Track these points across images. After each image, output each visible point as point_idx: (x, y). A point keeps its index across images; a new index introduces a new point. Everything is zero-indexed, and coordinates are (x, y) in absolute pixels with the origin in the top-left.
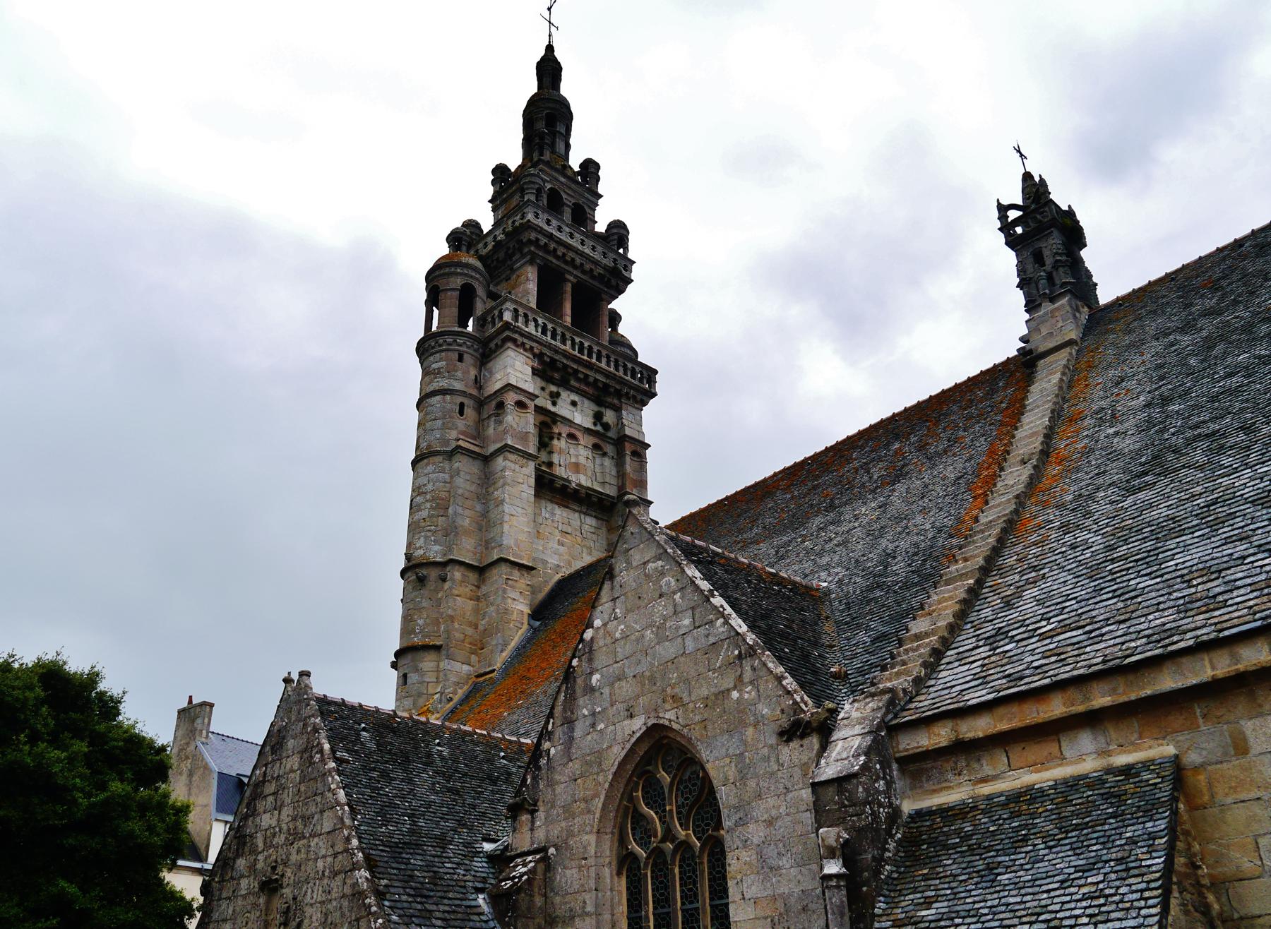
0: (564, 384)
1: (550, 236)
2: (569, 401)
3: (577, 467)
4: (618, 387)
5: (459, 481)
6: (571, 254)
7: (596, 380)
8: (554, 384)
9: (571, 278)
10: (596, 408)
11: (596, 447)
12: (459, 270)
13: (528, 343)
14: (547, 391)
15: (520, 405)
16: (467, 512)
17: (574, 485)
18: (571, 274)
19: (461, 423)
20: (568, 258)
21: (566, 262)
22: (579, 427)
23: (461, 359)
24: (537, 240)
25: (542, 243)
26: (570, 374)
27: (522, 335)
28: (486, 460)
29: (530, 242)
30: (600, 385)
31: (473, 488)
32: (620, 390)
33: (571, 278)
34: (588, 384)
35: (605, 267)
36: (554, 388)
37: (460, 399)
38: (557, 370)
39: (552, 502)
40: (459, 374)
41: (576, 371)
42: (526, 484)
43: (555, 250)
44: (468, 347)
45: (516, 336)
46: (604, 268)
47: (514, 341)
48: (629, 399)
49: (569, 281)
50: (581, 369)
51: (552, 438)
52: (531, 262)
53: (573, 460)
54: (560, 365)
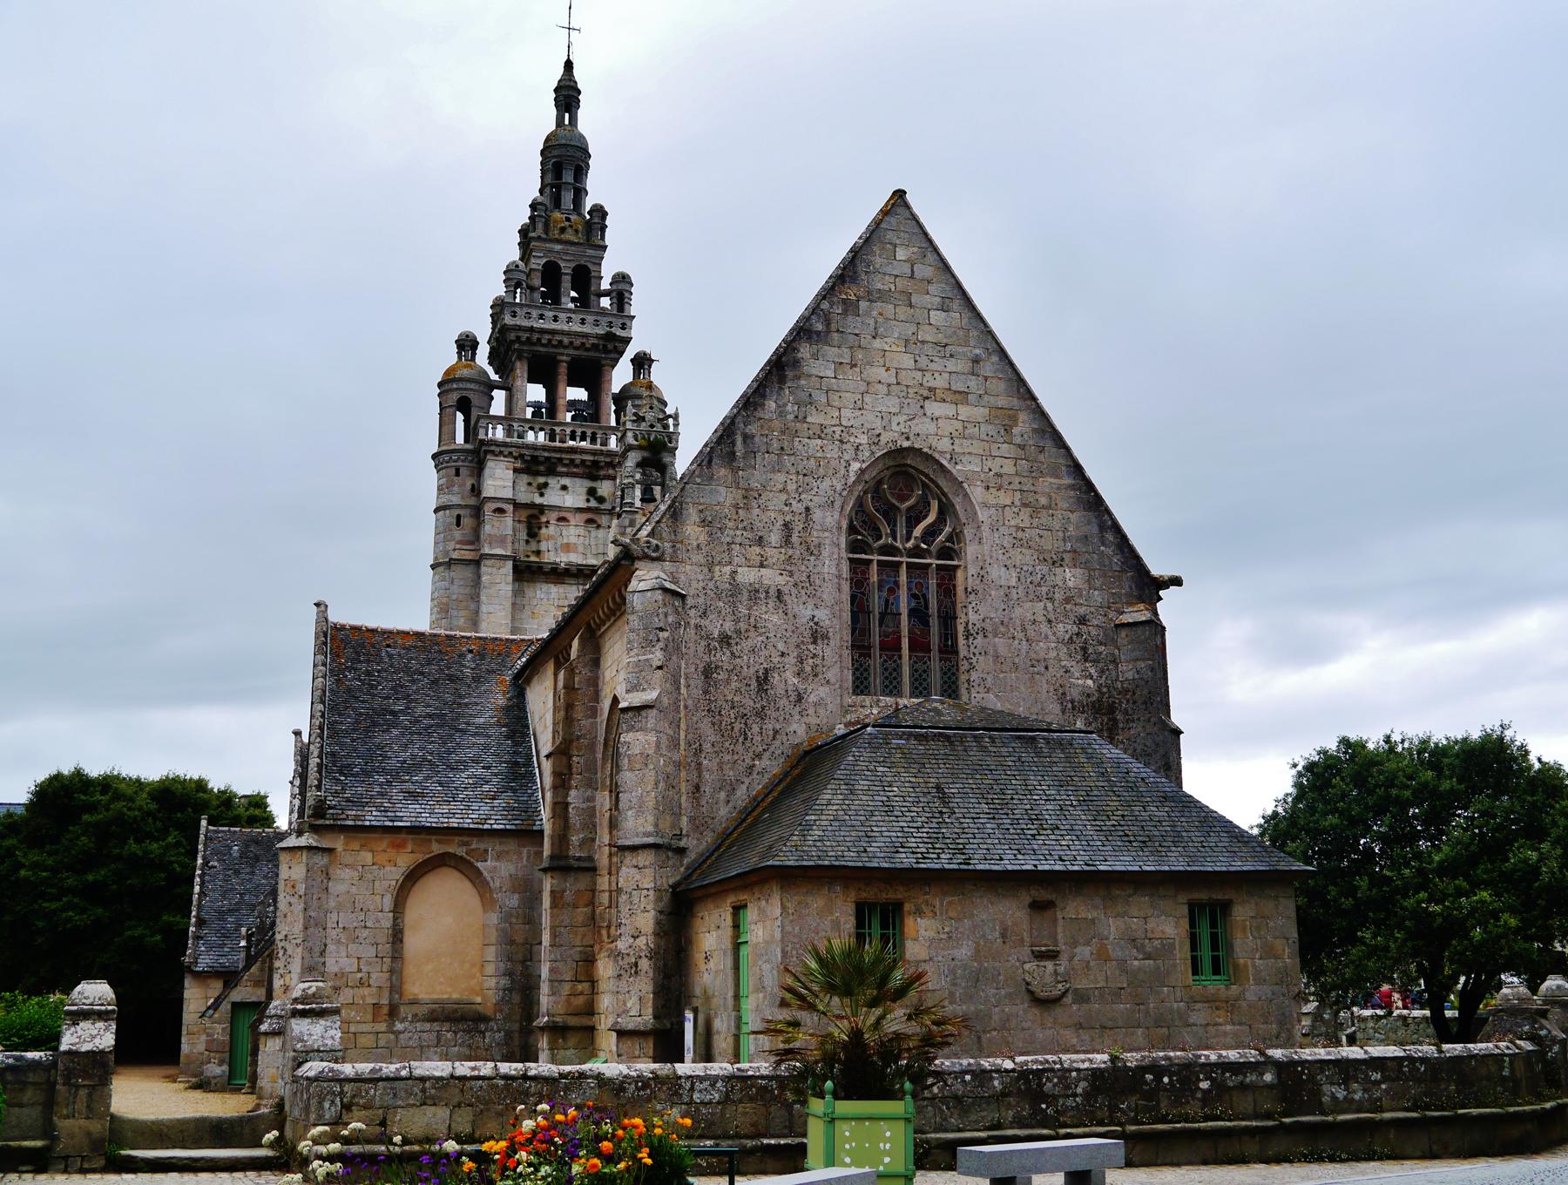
0: (552, 472)
1: (532, 329)
2: (559, 486)
3: (567, 548)
4: (608, 460)
5: (455, 588)
6: (558, 338)
7: (583, 461)
8: (541, 475)
9: (565, 358)
10: (588, 484)
11: (589, 521)
12: (455, 386)
13: (506, 451)
14: (535, 485)
15: (500, 511)
16: (462, 613)
17: (563, 565)
18: (562, 354)
19: (458, 534)
20: (554, 343)
21: (555, 347)
22: (569, 510)
23: (457, 474)
24: (518, 338)
25: (524, 339)
26: (555, 463)
27: (498, 446)
28: (477, 563)
29: (512, 342)
30: (588, 463)
31: (467, 591)
33: (565, 358)
34: (576, 466)
35: (597, 336)
36: (541, 480)
37: (457, 512)
38: (542, 463)
39: (547, 582)
40: (456, 489)
41: (560, 460)
42: (503, 584)
43: (539, 340)
44: (463, 461)
45: (493, 448)
47: (492, 452)
49: (562, 361)
50: (564, 456)
51: (540, 528)
52: (520, 358)
53: (565, 541)
54: (541, 459)
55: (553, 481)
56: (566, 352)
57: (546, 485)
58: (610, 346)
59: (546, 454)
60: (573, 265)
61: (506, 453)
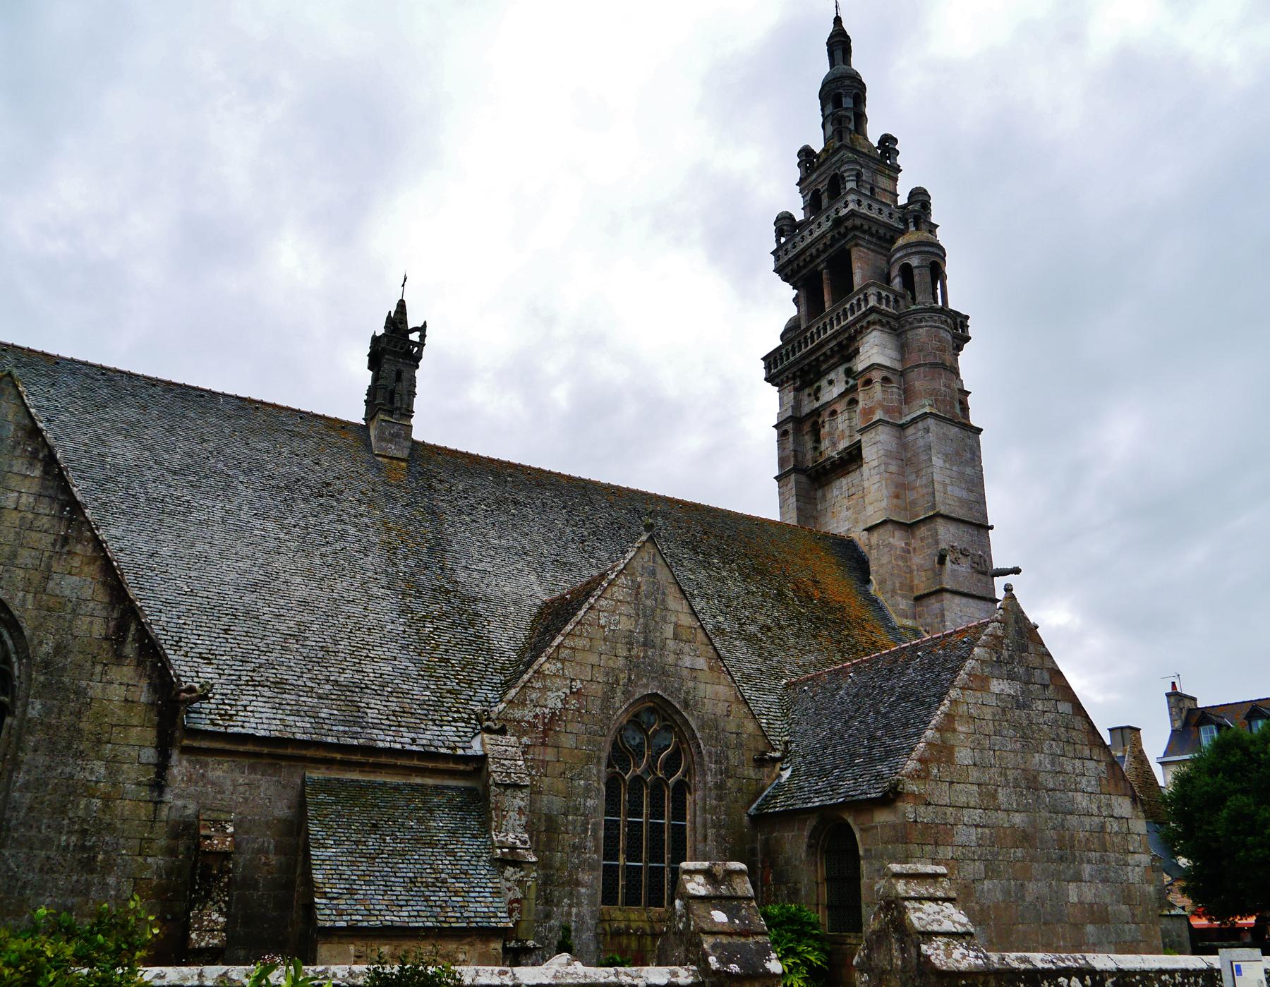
4: (846, 336)
7: (832, 349)
9: (822, 266)
18: (818, 264)
30: (836, 349)
32: (850, 334)
33: (822, 266)
34: (832, 357)
35: (831, 229)
41: (817, 359)
46: (831, 230)
48: (861, 332)
54: (806, 368)
55: (824, 383)
56: (819, 260)
57: (819, 389)
58: (842, 230)
59: (807, 361)
60: (827, 182)
61: (785, 379)
